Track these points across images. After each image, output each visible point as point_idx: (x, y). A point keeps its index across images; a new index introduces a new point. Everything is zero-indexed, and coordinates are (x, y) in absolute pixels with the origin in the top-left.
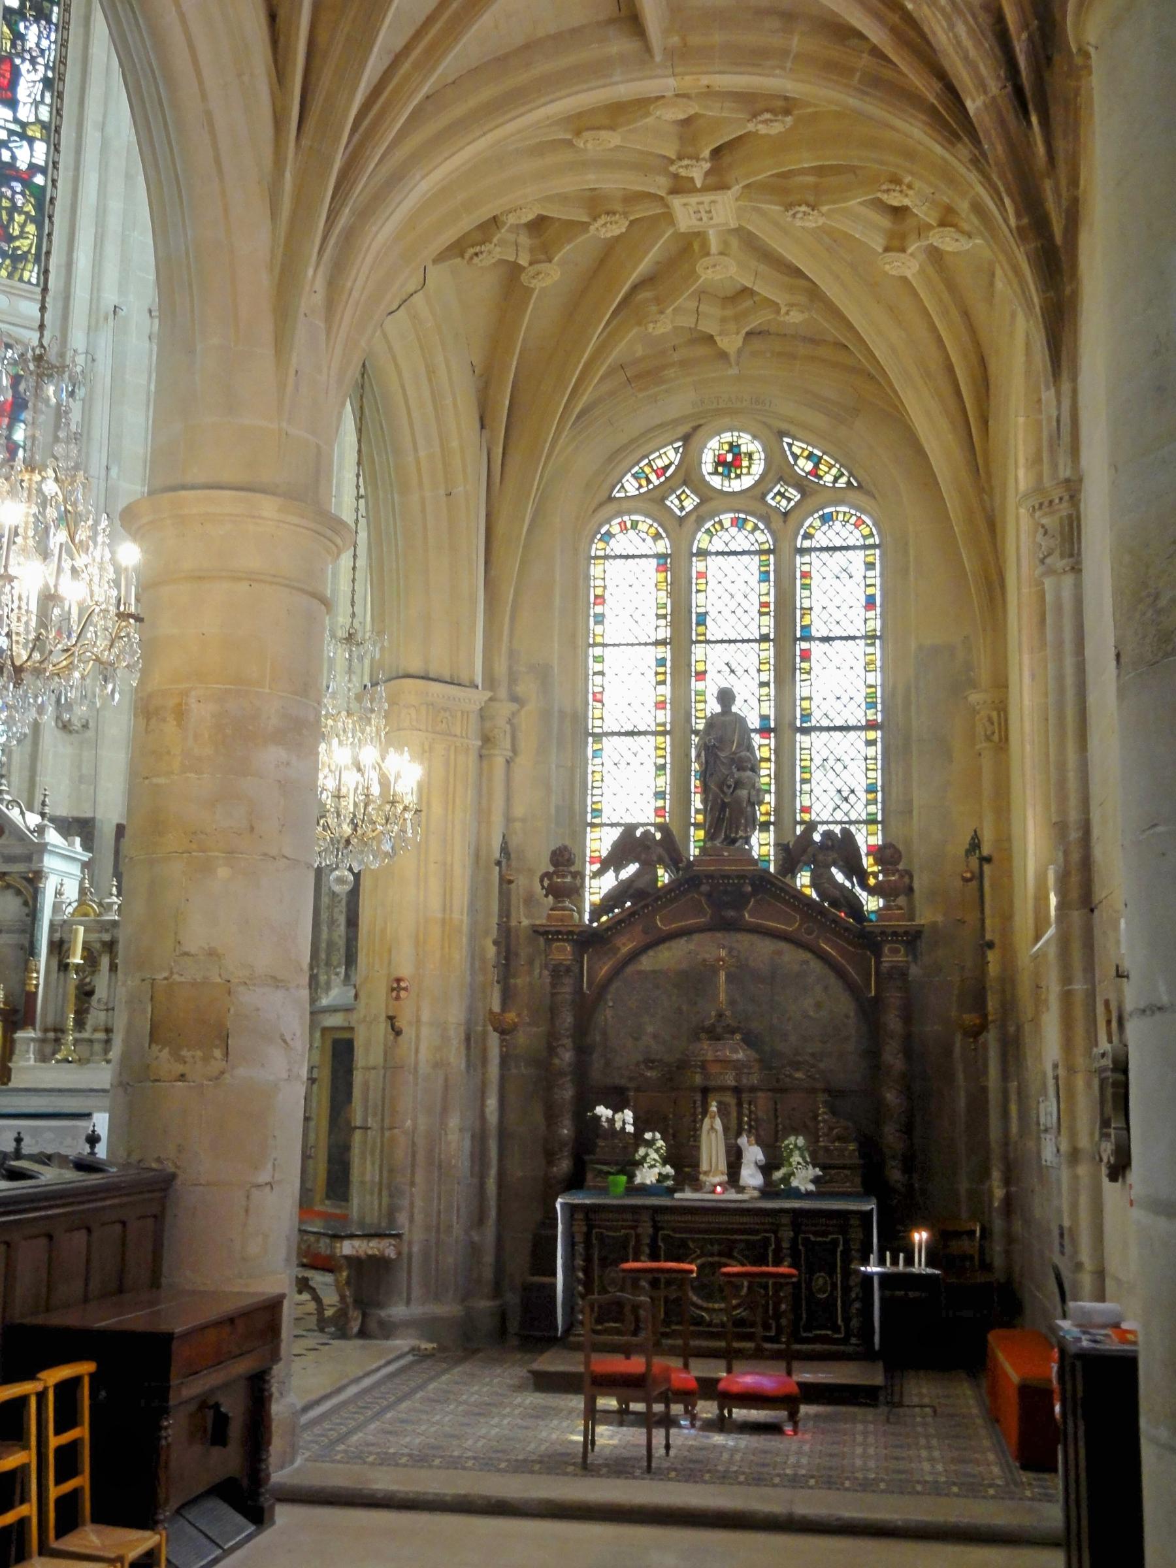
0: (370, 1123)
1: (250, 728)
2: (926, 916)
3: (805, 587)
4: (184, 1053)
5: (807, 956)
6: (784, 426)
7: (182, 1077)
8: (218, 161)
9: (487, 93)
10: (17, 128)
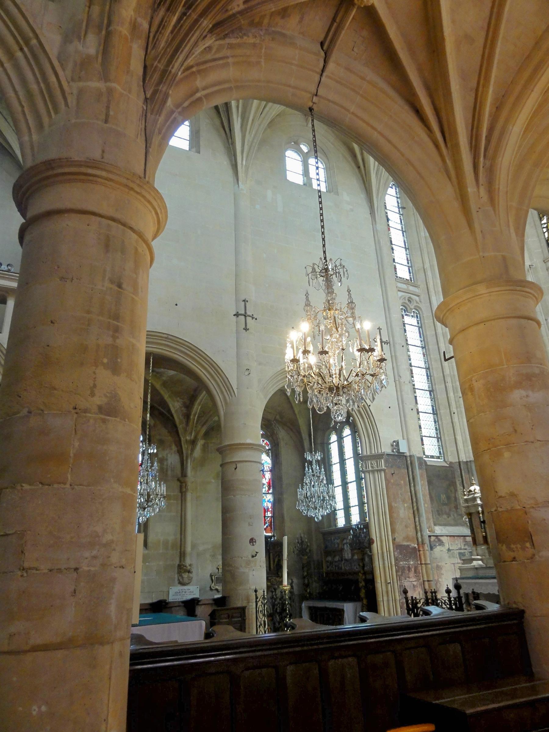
1: (502, 385)
4: (513, 546)
7: (514, 559)
8: (419, 173)
9: (526, 74)
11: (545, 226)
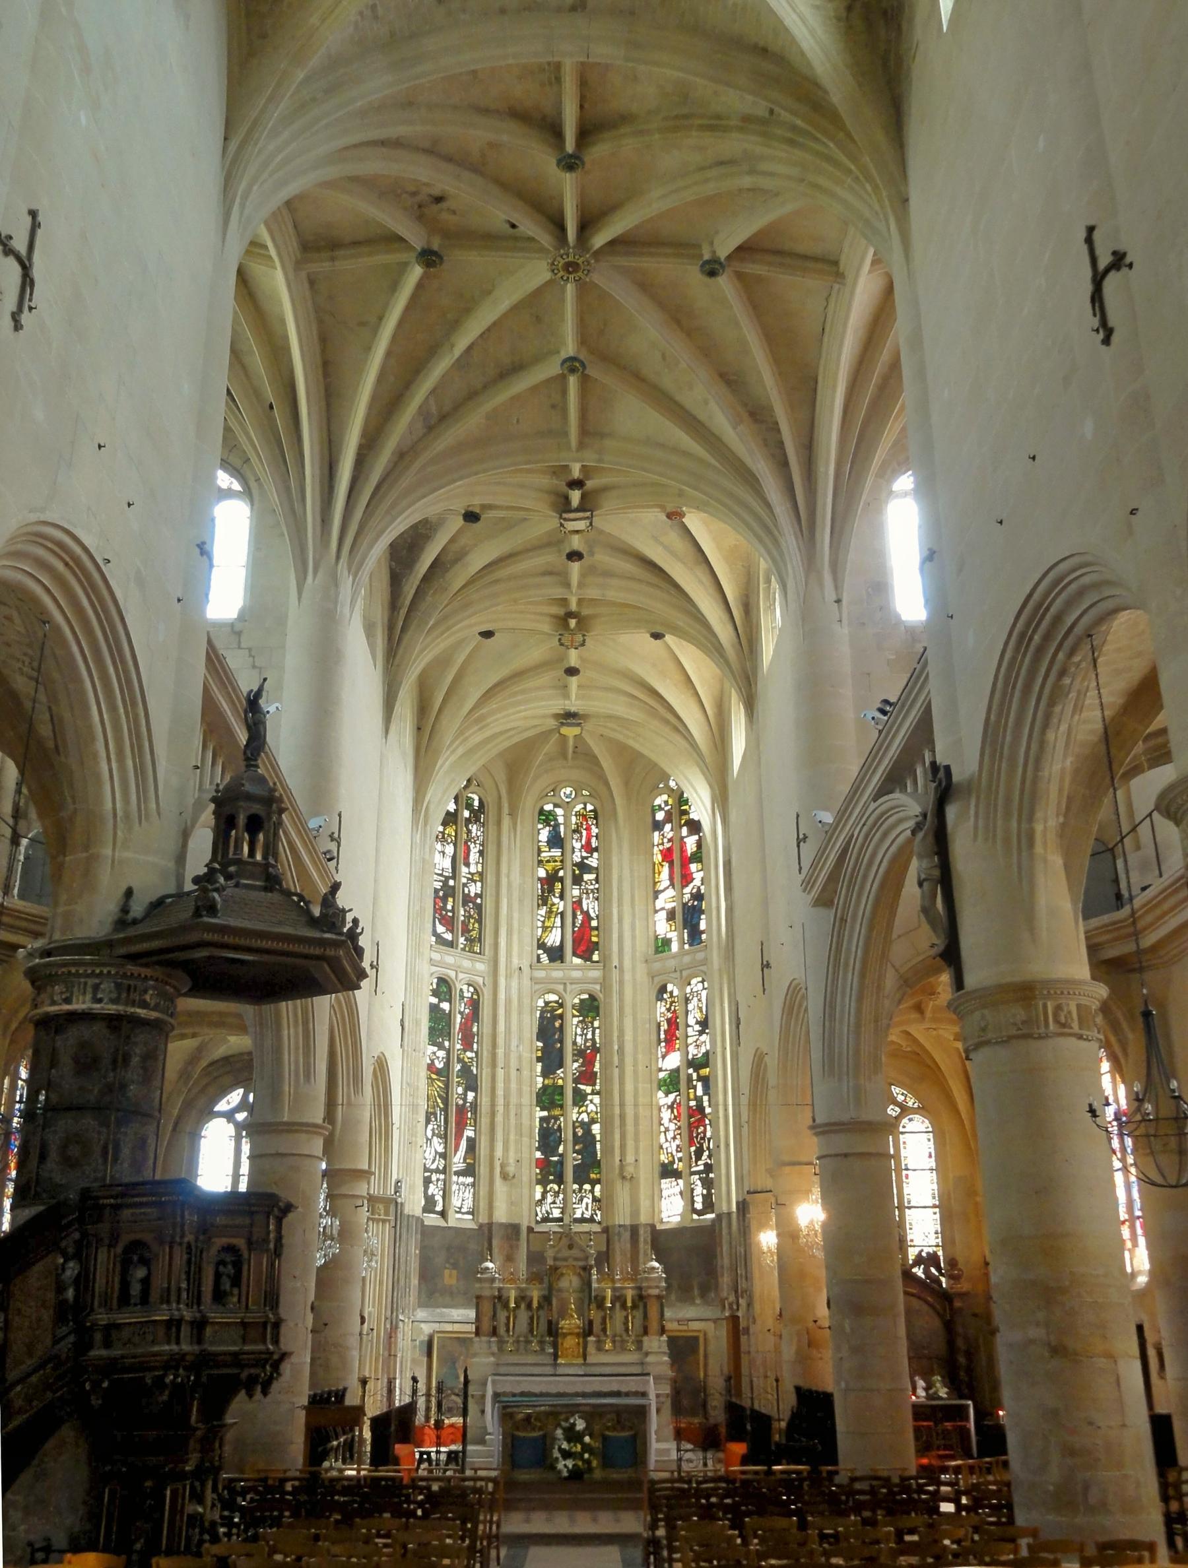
0: (769, 1374)
2: (964, 1286)
3: (905, 1148)
5: (921, 1302)
6: (892, 1081)
10: (470, 876)
11: (542, 919)
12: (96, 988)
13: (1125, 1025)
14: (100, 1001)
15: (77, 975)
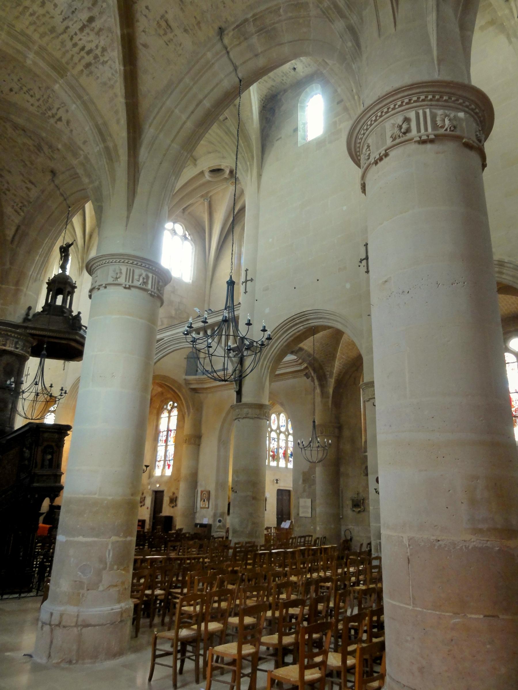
12: (17, 343)
13: (191, 408)
14: (17, 348)
15: (11, 336)
